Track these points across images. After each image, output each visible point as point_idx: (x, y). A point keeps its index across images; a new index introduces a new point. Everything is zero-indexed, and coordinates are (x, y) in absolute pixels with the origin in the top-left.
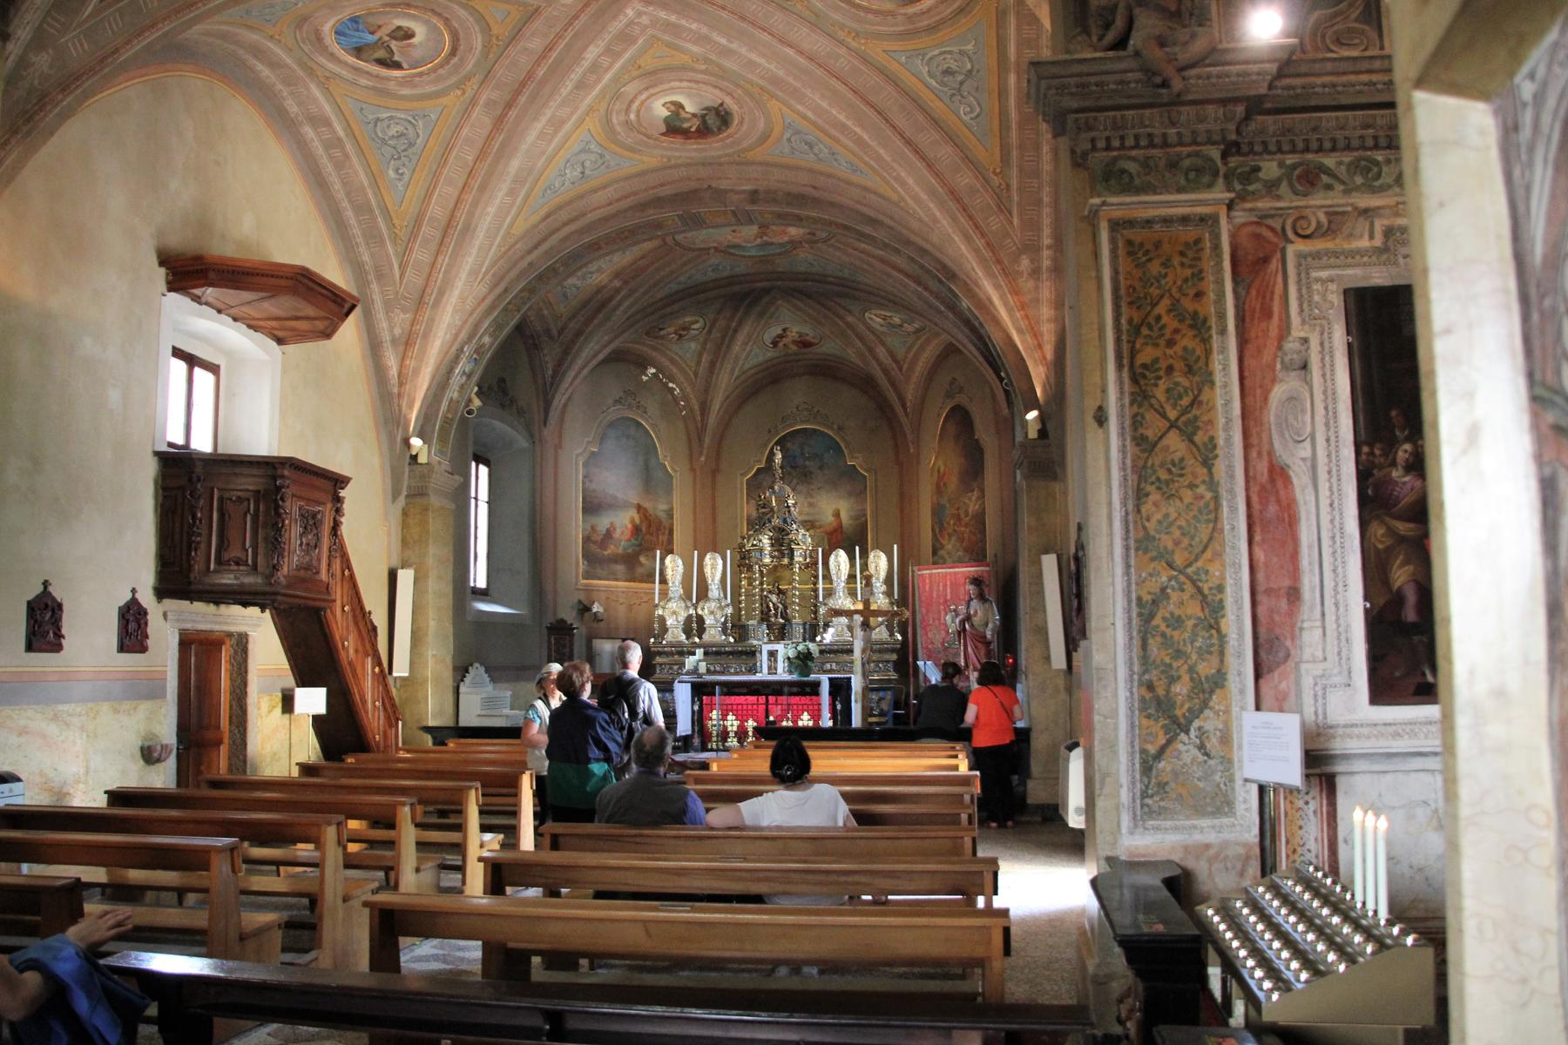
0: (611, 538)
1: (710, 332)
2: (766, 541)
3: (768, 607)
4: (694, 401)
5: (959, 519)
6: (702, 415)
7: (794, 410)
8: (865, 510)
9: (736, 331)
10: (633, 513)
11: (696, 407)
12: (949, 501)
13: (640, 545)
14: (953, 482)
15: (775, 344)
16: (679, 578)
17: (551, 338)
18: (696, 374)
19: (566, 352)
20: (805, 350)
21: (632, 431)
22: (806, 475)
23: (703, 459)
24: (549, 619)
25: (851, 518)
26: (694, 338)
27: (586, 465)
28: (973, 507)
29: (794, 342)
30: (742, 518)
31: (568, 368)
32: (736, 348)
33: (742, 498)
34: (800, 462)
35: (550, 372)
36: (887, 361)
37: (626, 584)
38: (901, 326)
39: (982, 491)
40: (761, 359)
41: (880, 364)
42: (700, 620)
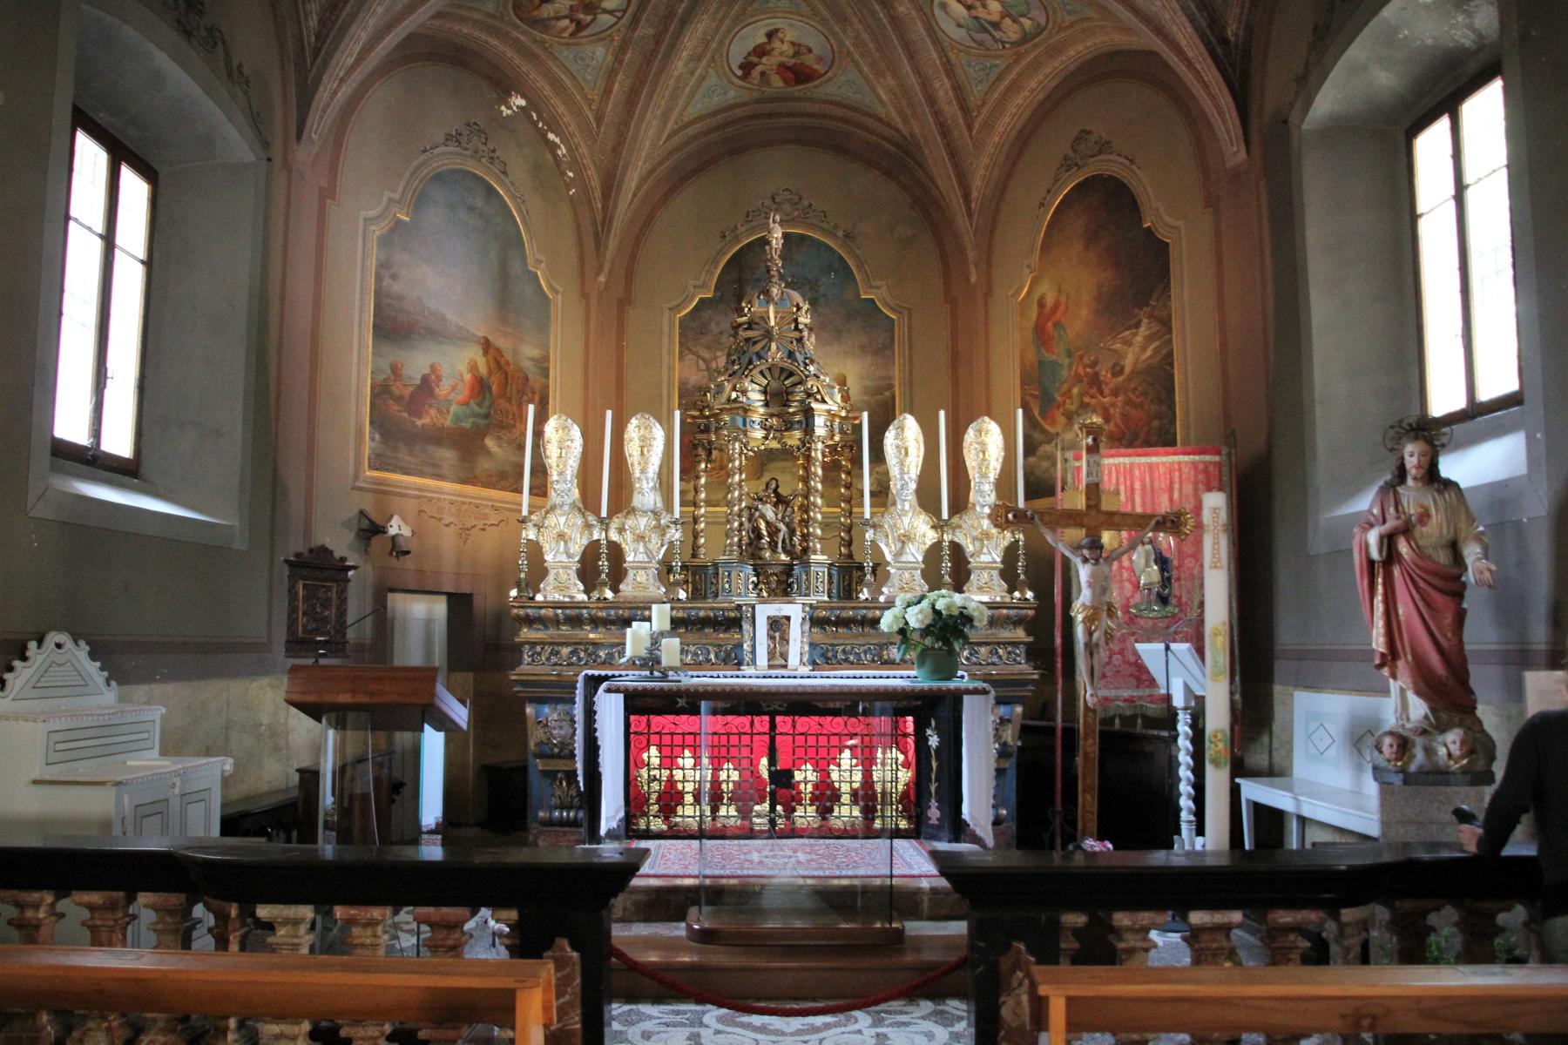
0: (431, 393)
1: (635, 21)
2: (755, 397)
3: (756, 530)
4: (592, 172)
5: (1095, 381)
6: (606, 197)
7: (768, 202)
8: (890, 378)
9: (684, 23)
10: (474, 354)
11: (596, 183)
12: (1069, 354)
13: (487, 416)
14: (1079, 319)
15: (747, 67)
16: (573, 462)
18: (599, 119)
20: (797, 90)
21: (479, 201)
23: (602, 278)
24: (295, 546)
25: (866, 390)
26: (600, 37)
27: (385, 242)
28: (1135, 350)
29: (782, 67)
30: (670, 383)
32: (679, 66)
33: (670, 351)
35: (313, 23)
36: (951, 110)
37: (458, 487)
38: (996, 25)
39: (1166, 324)
40: (716, 101)
41: (937, 114)
42: (616, 552)
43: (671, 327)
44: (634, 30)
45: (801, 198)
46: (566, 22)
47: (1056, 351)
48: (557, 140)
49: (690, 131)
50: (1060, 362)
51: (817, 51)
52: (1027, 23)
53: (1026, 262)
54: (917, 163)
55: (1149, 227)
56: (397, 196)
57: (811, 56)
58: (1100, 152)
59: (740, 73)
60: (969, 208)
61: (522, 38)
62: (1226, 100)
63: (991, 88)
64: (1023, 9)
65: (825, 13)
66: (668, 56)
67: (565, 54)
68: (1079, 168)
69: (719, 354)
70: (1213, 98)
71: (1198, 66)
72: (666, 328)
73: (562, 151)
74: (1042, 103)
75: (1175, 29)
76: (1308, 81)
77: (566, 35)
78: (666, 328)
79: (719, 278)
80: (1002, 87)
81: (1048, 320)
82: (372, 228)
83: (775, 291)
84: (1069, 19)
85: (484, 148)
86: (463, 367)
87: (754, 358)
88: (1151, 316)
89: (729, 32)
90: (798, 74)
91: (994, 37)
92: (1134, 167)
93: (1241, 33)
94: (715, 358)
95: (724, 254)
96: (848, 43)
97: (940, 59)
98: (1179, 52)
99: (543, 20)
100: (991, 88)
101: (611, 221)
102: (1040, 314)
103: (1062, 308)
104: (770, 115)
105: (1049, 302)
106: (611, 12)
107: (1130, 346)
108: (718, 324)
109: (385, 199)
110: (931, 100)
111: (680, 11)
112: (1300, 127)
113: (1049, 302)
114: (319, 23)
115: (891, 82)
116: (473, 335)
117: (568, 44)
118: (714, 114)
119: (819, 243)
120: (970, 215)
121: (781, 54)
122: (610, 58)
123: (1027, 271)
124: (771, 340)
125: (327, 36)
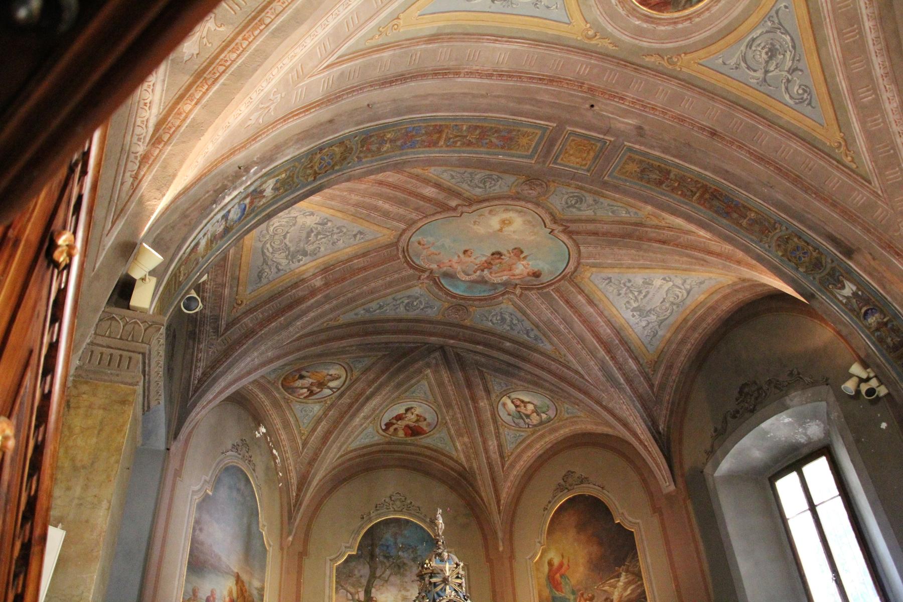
1: (341, 396)
6: (299, 490)
7: (388, 500)
9: (368, 399)
11: (294, 481)
12: (573, 592)
15: (388, 425)
17: (216, 330)
18: (305, 444)
19: (227, 353)
20: (409, 439)
21: (242, 485)
22: (399, 567)
23: (290, 539)
26: (319, 401)
27: (200, 507)
29: (407, 426)
31: (224, 373)
32: (357, 420)
33: (331, 588)
34: (393, 552)
35: (199, 373)
36: (495, 456)
38: (528, 416)
39: (638, 575)
40: (367, 441)
41: (488, 458)
43: (331, 572)
44: (339, 399)
45: (405, 499)
46: (306, 390)
47: (564, 590)
48: (277, 454)
49: (348, 457)
50: (567, 597)
51: (429, 420)
52: (544, 416)
53: (537, 540)
54: (471, 485)
55: (619, 523)
56: (208, 478)
57: (425, 423)
58: (582, 483)
59: (384, 427)
60: (499, 510)
61: (277, 395)
62: (661, 460)
63: (516, 448)
64: (544, 409)
65: (441, 403)
66: (354, 415)
67: (297, 407)
68: (569, 490)
69: (360, 590)
70: (654, 459)
71: (646, 444)
72: (328, 573)
73: (278, 461)
74: (540, 456)
75: (635, 425)
76: (714, 452)
77: (302, 397)
78: (328, 573)
79: (360, 542)
80: (524, 445)
81: (556, 573)
82: (195, 497)
83: (446, 554)
84: (567, 416)
85: (246, 454)
86: (226, 593)
87: (436, 595)
88: (627, 571)
89: (387, 406)
90: (414, 431)
91: (525, 421)
92: (604, 491)
93: (666, 429)
94: (358, 592)
95: (363, 528)
96: (447, 418)
97: (495, 430)
98: (635, 435)
99: (293, 388)
100: (516, 448)
101: (301, 505)
102: (550, 571)
103: (565, 565)
104: (391, 451)
105: (556, 562)
106: (331, 389)
107: (615, 588)
108: (359, 571)
109: (203, 480)
110: (486, 451)
111: (368, 393)
112: (712, 475)
113: (556, 562)
114: (202, 373)
115: (466, 439)
116: (232, 572)
117: (301, 402)
118: (363, 448)
119: (416, 524)
120: (499, 513)
121: (409, 420)
122: (321, 413)
123: (538, 544)
124: (446, 584)
125: (205, 381)
